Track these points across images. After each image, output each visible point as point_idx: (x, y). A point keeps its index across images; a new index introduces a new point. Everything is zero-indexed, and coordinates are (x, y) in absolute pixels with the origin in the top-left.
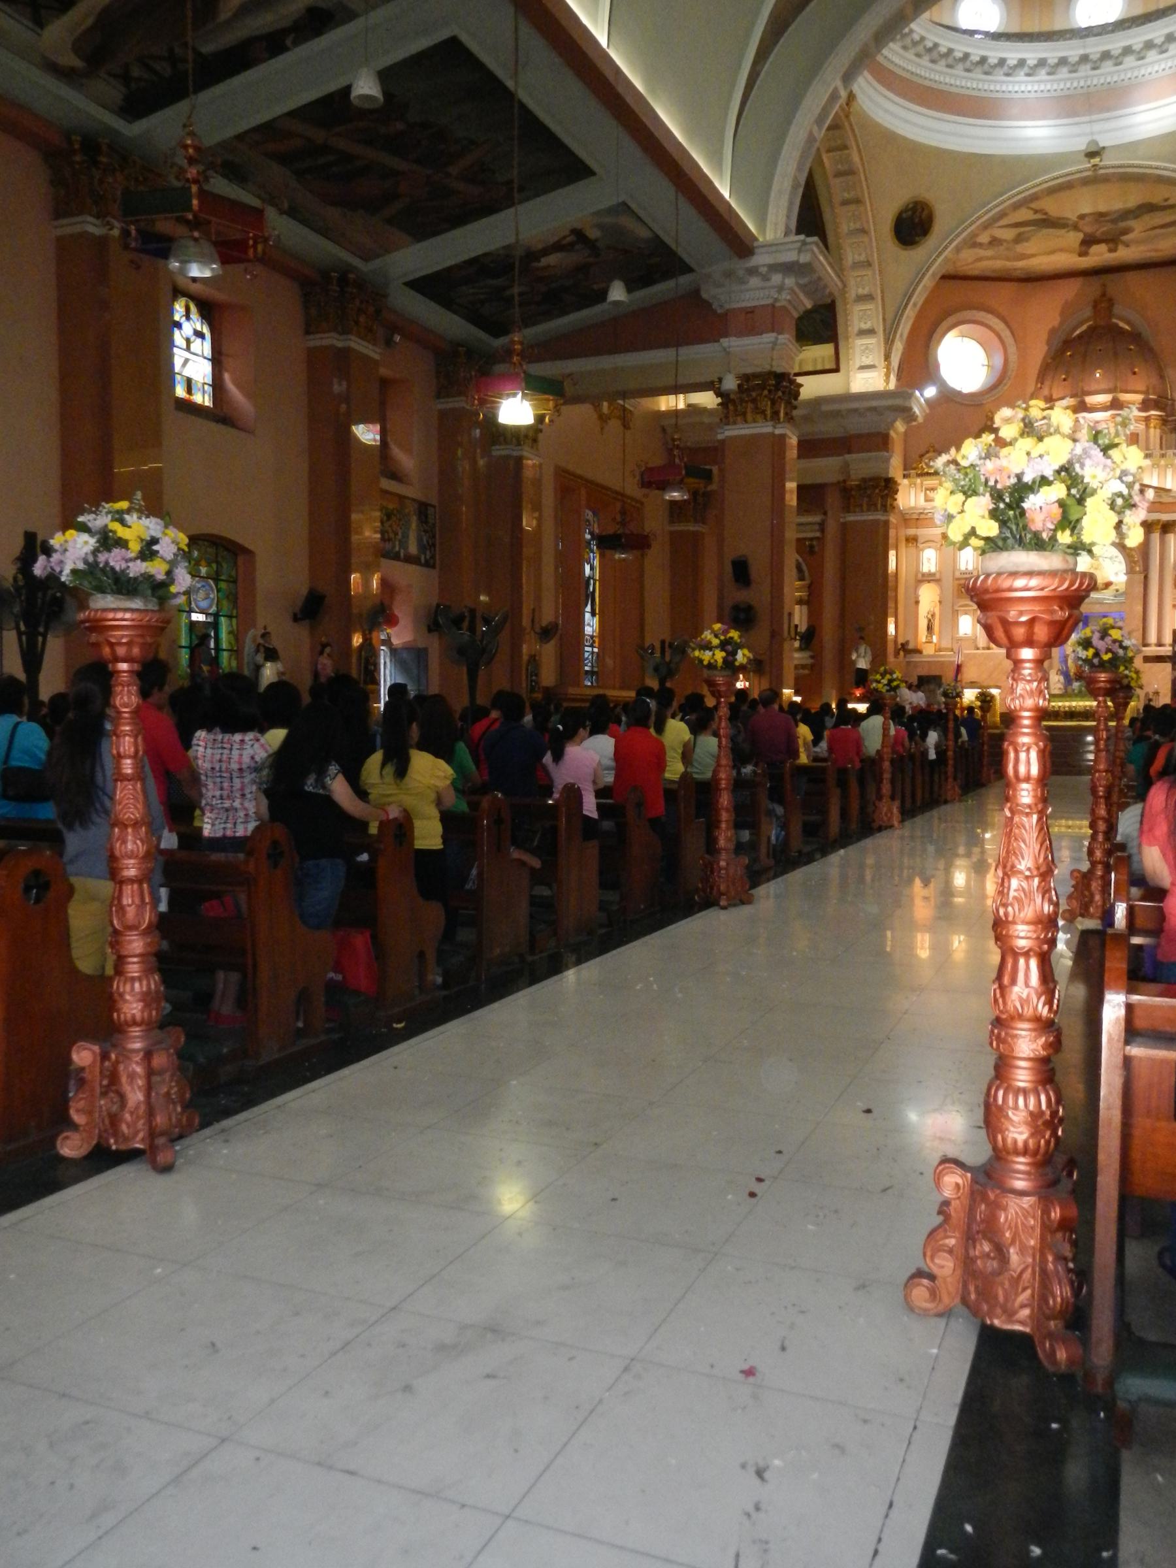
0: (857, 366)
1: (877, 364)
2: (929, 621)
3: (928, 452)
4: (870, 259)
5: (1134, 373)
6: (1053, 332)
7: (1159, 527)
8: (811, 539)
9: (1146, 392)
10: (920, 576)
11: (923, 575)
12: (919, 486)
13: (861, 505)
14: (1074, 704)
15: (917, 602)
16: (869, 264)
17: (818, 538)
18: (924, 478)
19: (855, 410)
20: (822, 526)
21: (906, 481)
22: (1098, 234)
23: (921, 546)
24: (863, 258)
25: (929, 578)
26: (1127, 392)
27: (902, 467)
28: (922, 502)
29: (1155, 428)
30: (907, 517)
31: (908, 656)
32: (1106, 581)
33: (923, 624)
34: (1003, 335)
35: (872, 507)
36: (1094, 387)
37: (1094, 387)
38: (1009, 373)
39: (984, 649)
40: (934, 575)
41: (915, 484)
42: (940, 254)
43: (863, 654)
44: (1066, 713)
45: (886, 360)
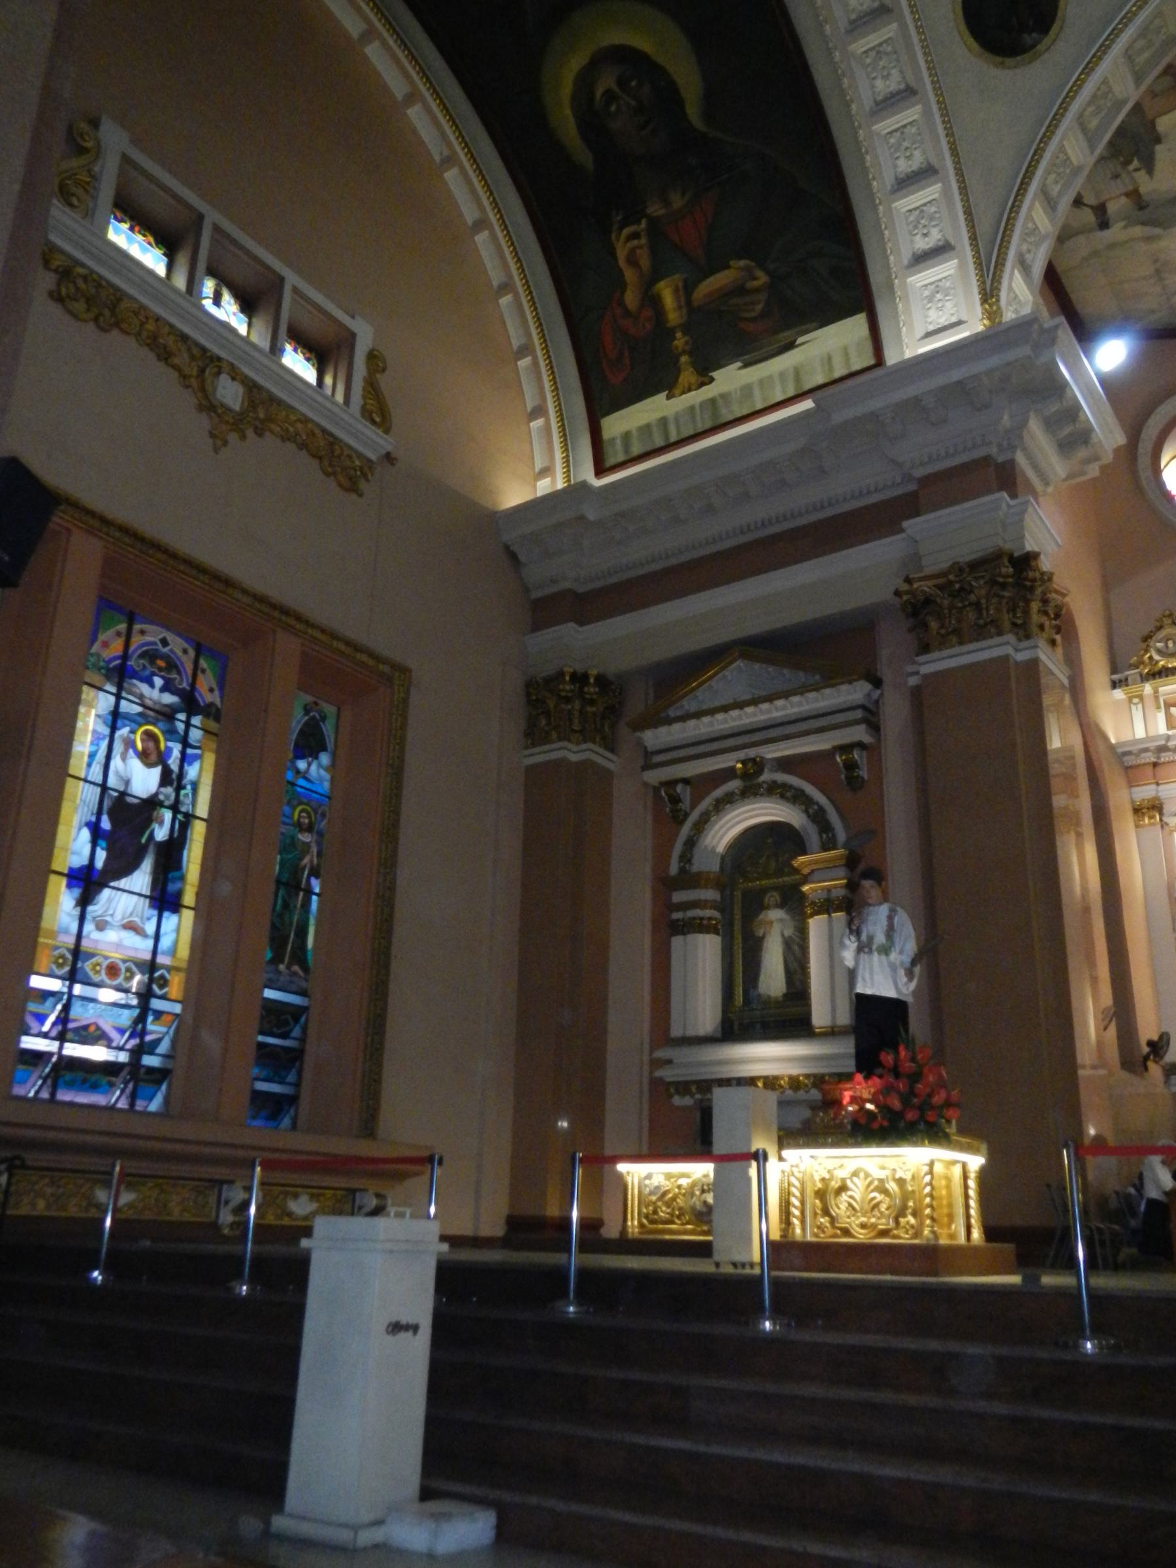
0: (920, 332)
1: (964, 318)
3: (1160, 628)
4: (913, 84)
8: (845, 749)
16: (908, 93)
17: (860, 745)
18: (1158, 681)
19: (916, 402)
20: (871, 716)
21: (1119, 694)
24: (894, 84)
28: (1161, 728)
30: (1130, 761)
35: (983, 630)
41: (1141, 698)
42: (1089, 69)
43: (880, 938)
45: (984, 301)
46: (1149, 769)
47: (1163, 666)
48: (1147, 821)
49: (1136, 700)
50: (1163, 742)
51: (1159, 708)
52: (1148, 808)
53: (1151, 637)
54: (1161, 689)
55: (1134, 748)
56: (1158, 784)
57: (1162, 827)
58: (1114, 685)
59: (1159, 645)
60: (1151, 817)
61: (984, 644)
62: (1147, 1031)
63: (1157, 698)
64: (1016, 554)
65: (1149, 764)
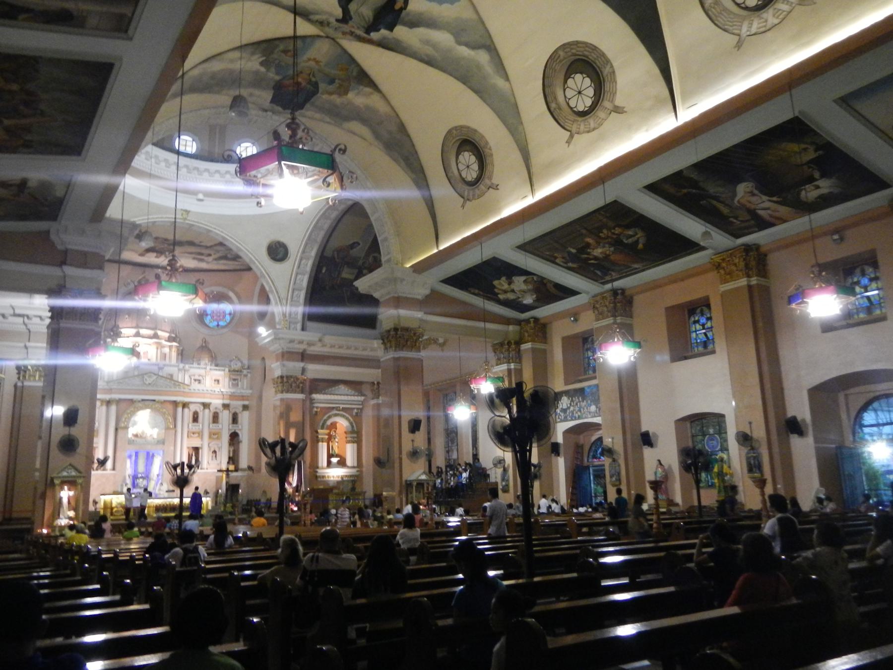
9: (170, 332)
13: (35, 377)
22: (157, 248)
37: (145, 325)
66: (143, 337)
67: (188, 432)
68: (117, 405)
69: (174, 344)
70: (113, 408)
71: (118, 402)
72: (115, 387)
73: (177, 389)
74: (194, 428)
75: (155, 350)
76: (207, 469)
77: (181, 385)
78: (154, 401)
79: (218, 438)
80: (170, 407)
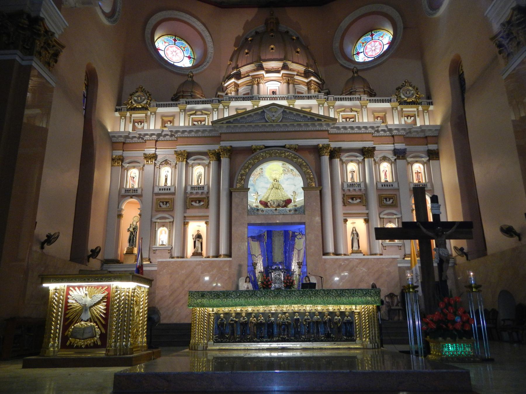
2: (131, 233)
3: (137, 92)
5: (298, 52)
6: (238, 38)
7: (328, 151)
9: (307, 66)
10: (123, 192)
11: (127, 191)
12: (128, 120)
14: (273, 308)
15: (120, 216)
21: (117, 114)
23: (126, 165)
25: (132, 193)
26: (293, 62)
27: (116, 104)
28: (130, 130)
29: (315, 91)
30: (114, 140)
31: (105, 266)
32: (285, 199)
33: (125, 236)
34: (204, 35)
36: (268, 57)
38: (208, 60)
39: (178, 257)
40: (136, 190)
41: (125, 117)
44: (259, 325)
46: (122, 144)
47: (135, 107)
48: (116, 164)
49: (123, 118)
50: (127, 134)
51: (131, 122)
52: (118, 159)
53: (133, 94)
54: (133, 115)
55: (116, 135)
56: (123, 151)
57: (122, 167)
58: (116, 110)
59: (136, 98)
60: (118, 163)
61: (6, 52)
62: (92, 245)
63: (130, 118)
64: (33, 15)
65: (121, 142)
66: (268, 71)
67: (344, 195)
68: (230, 158)
69: (313, 78)
70: (225, 161)
71: (232, 152)
72: (224, 130)
73: (318, 128)
74: (351, 189)
75: (285, 85)
76: (381, 255)
77: (323, 120)
78: (284, 147)
79: (394, 205)
80: (311, 158)
